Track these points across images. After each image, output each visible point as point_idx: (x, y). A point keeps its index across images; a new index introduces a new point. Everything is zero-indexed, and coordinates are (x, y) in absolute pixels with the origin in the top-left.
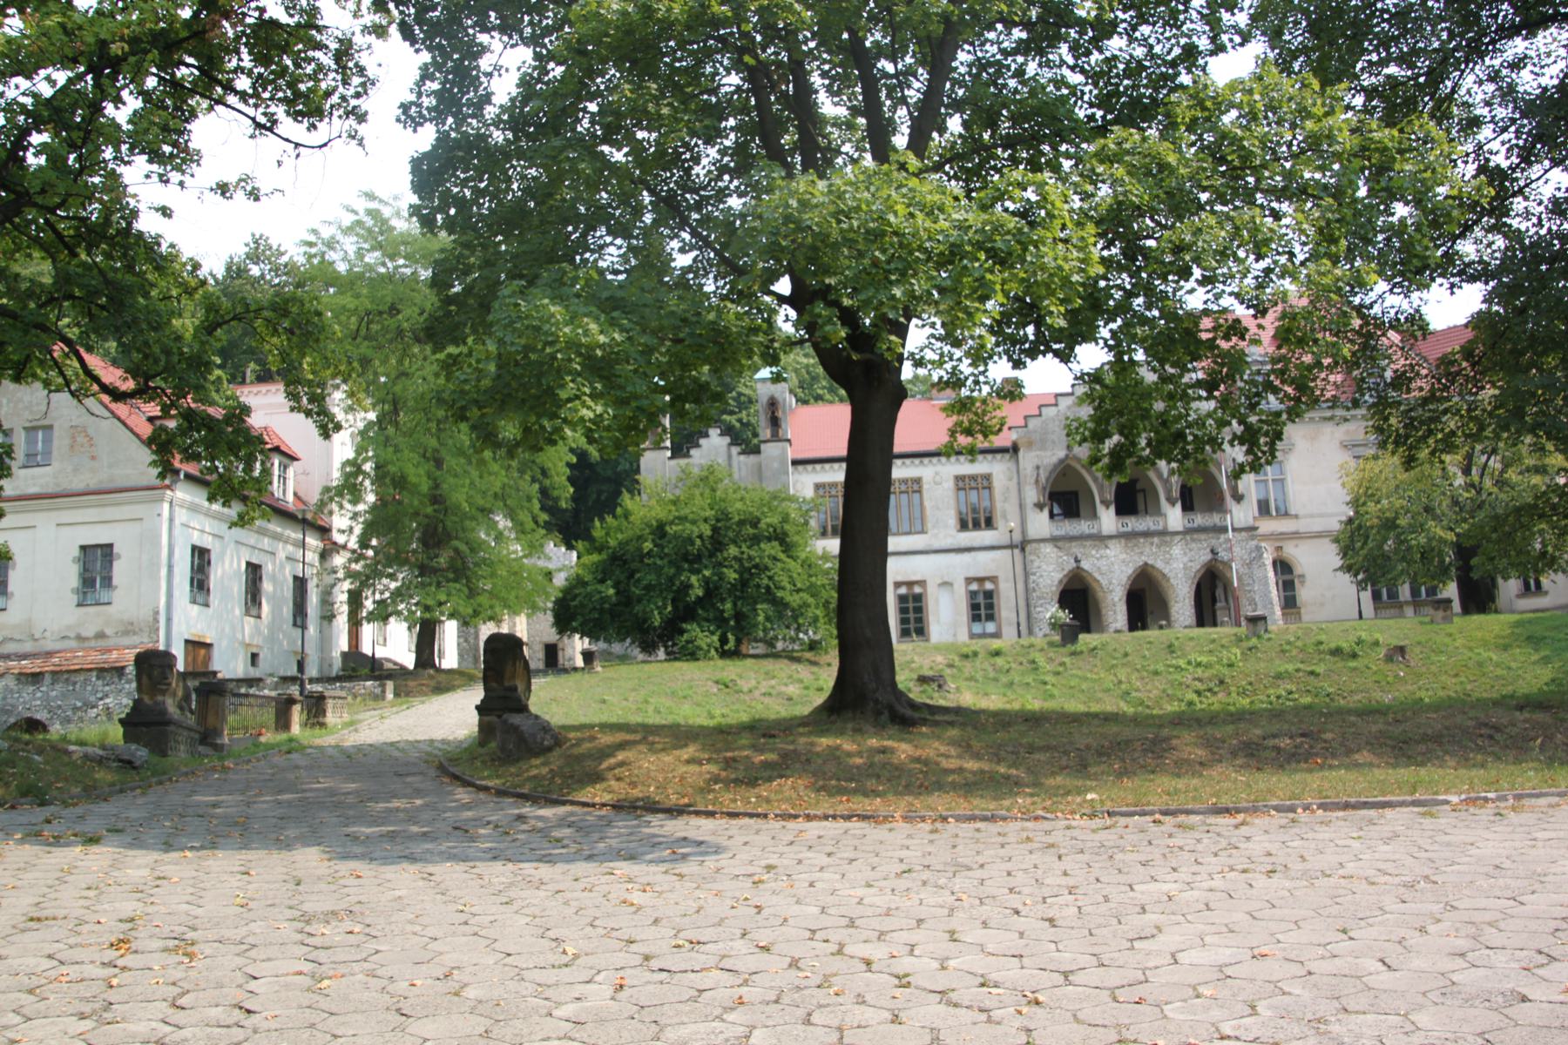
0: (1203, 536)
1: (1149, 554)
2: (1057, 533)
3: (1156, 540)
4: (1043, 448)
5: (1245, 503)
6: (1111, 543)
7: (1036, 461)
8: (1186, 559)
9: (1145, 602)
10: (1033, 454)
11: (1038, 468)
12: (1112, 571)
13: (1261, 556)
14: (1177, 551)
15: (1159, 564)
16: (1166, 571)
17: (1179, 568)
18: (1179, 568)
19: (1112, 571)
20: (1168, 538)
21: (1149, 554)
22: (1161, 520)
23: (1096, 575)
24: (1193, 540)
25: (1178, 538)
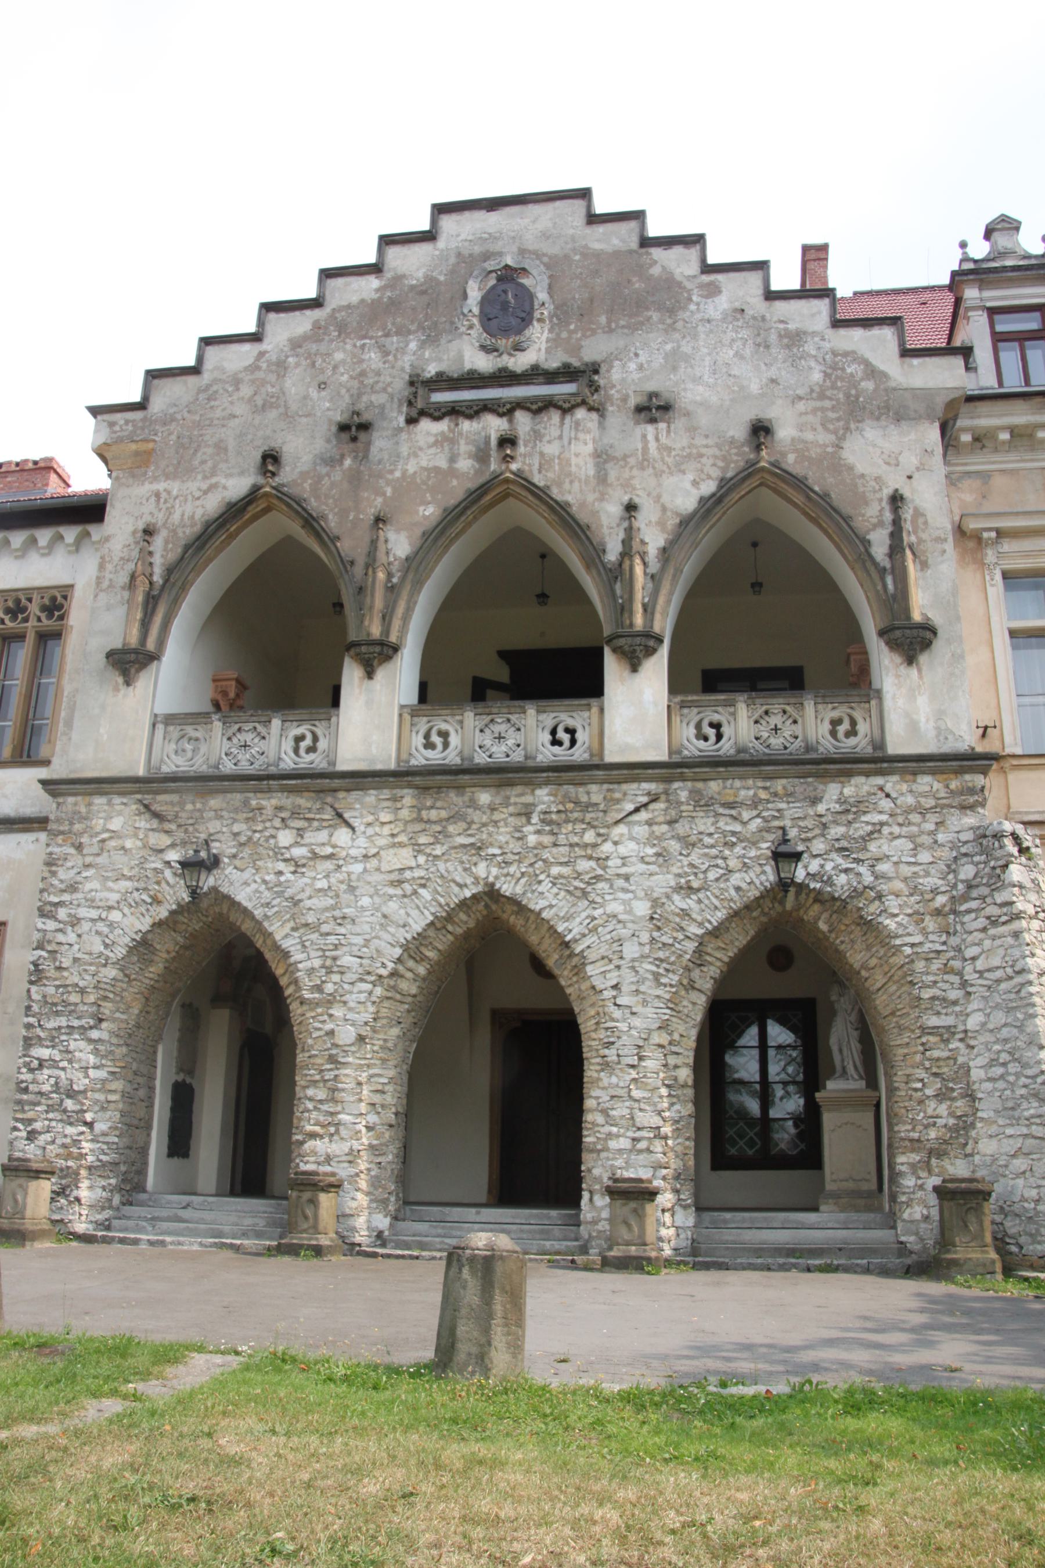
0: (745, 789)
1: (513, 855)
2: (174, 763)
3: (543, 797)
4: (181, 470)
5: (934, 662)
6: (361, 807)
7: (150, 513)
8: (663, 881)
9: (507, 1057)
10: (147, 488)
11: (149, 532)
12: (354, 909)
13: (997, 877)
14: (628, 844)
15: (547, 900)
16: (572, 929)
17: (634, 916)
18: (634, 916)
19: (354, 909)
20: (596, 793)
21: (513, 855)
22: (574, 716)
23: (280, 931)
24: (702, 803)
25: (638, 791)
